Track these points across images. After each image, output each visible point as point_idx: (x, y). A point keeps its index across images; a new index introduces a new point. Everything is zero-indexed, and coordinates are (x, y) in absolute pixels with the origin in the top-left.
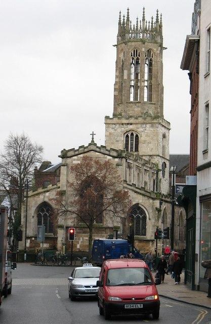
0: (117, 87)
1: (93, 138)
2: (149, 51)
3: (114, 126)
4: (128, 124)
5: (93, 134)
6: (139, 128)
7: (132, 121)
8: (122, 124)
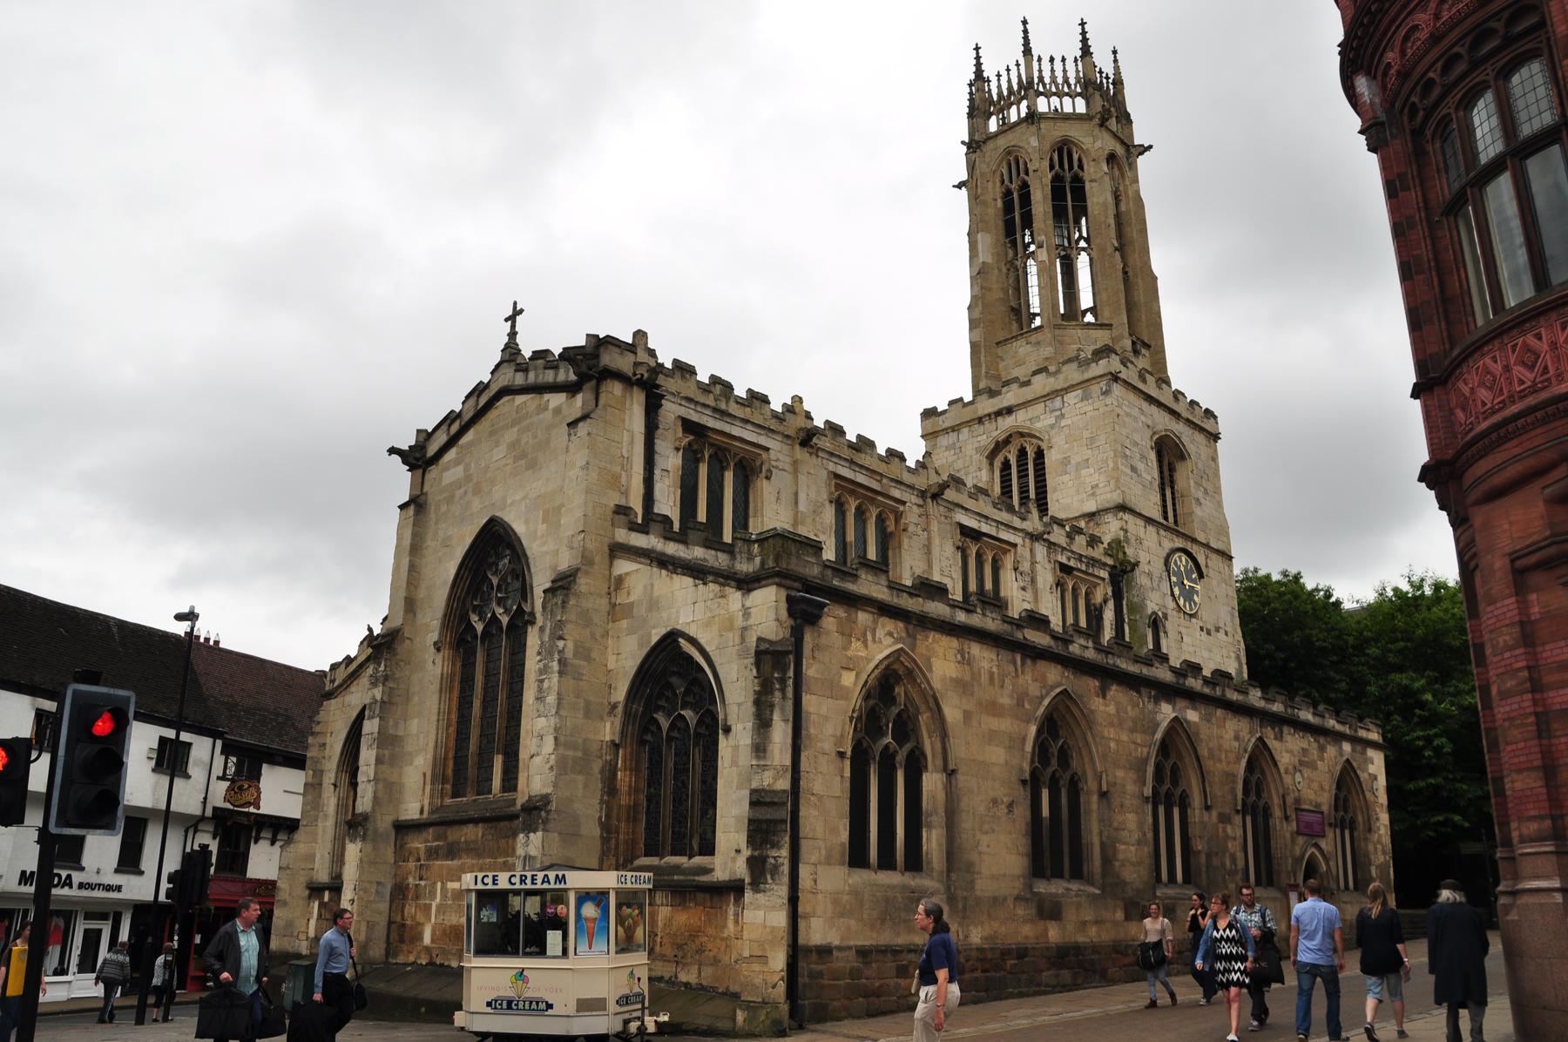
1: (513, 334)
2: (1064, 150)
3: (952, 437)
4: (999, 413)
5: (517, 312)
6: (1038, 418)
7: (1010, 397)
8: (980, 420)
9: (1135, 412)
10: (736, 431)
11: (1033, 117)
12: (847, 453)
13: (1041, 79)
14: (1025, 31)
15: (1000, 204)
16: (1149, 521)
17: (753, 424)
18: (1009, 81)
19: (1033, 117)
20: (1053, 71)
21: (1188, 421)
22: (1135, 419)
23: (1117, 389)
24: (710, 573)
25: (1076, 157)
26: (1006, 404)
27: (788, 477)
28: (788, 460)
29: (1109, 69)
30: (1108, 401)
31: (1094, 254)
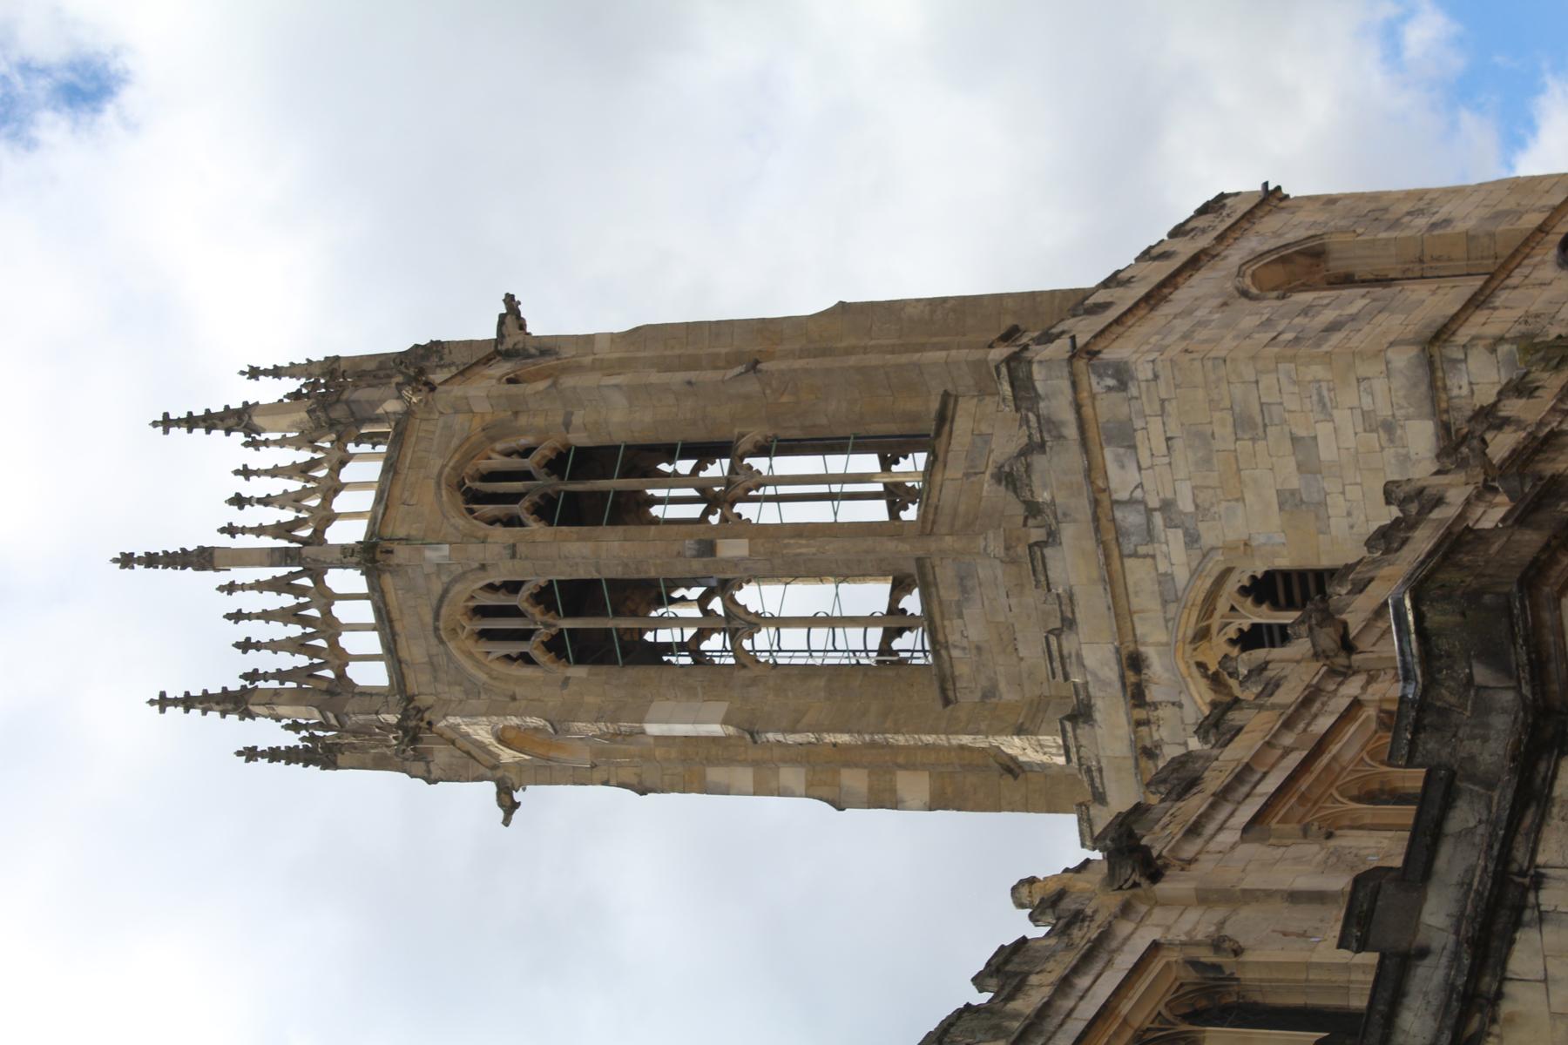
0: (855, 780)
4: (1137, 696)
6: (1165, 579)
7: (1096, 658)
9: (1182, 325)
10: (1088, 1009)
11: (368, 556)
12: (1195, 804)
13: (281, 530)
14: (151, 560)
15: (579, 672)
16: (1476, 302)
17: (1076, 970)
18: (266, 616)
19: (368, 556)
20: (266, 501)
21: (1221, 238)
22: (1202, 324)
23: (1113, 352)
24: (1505, 857)
25: (498, 462)
26: (1111, 673)
27: (1247, 912)
28: (1192, 916)
29: (292, 385)
30: (1143, 372)
31: (757, 434)
